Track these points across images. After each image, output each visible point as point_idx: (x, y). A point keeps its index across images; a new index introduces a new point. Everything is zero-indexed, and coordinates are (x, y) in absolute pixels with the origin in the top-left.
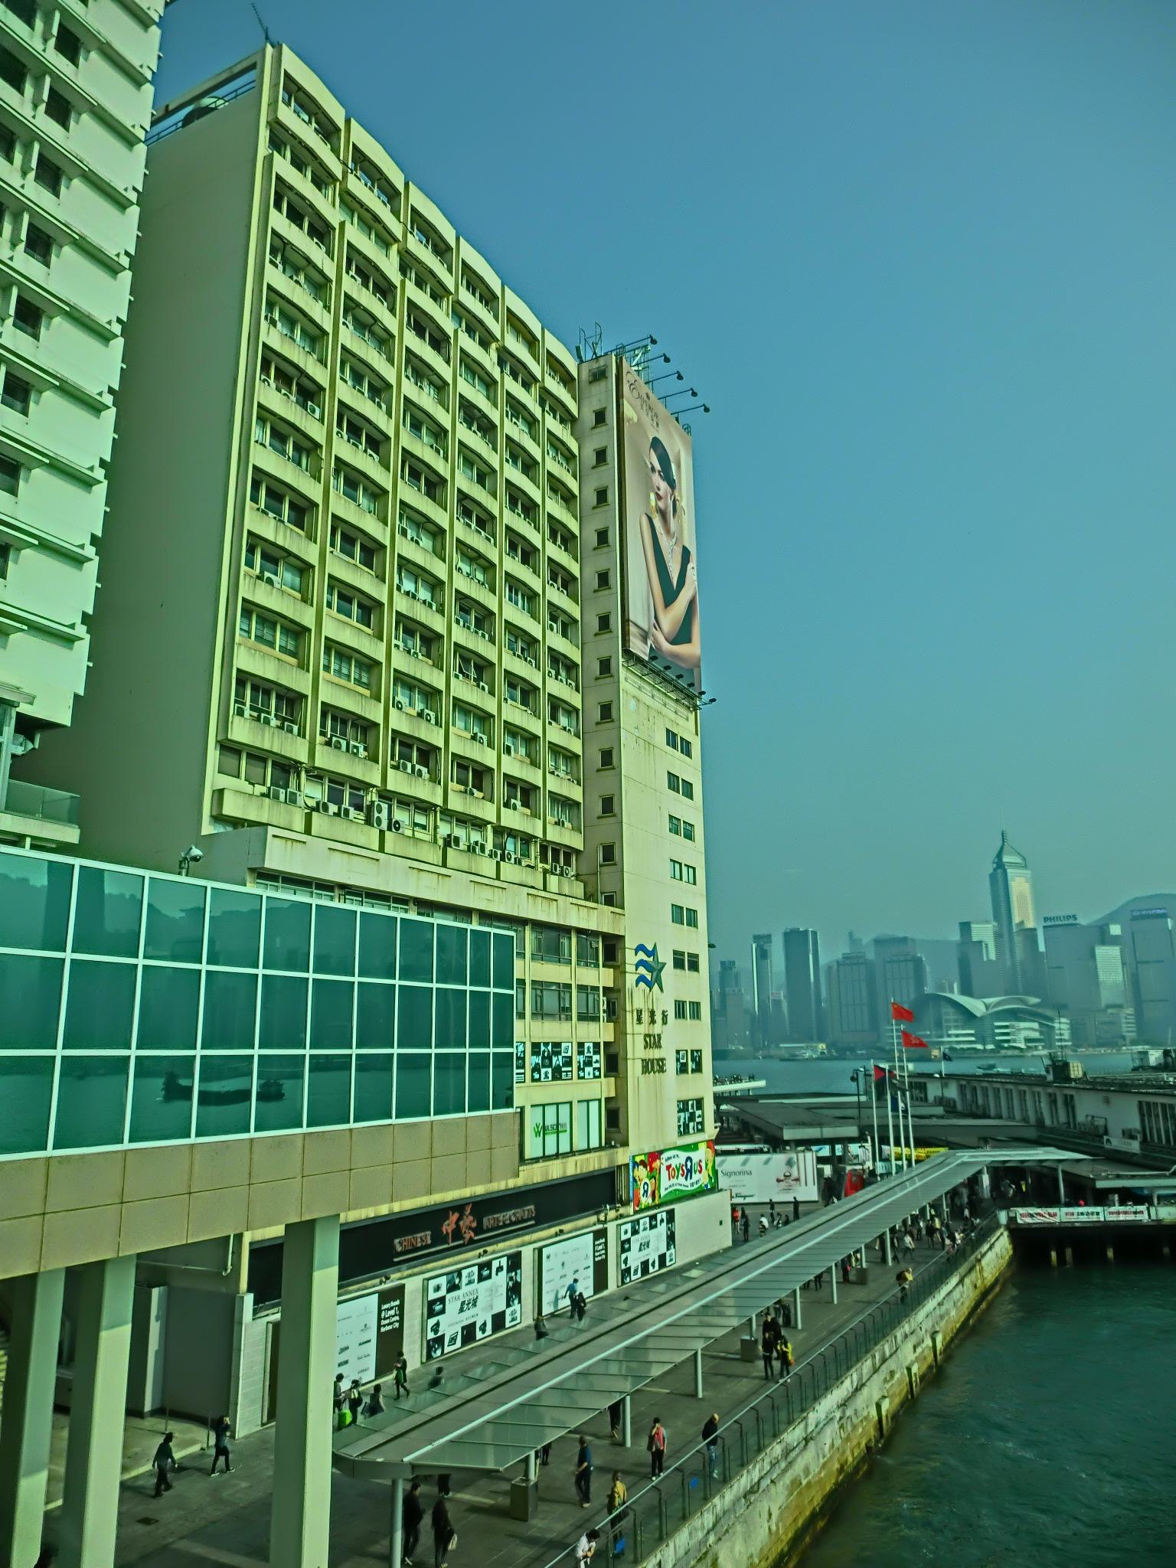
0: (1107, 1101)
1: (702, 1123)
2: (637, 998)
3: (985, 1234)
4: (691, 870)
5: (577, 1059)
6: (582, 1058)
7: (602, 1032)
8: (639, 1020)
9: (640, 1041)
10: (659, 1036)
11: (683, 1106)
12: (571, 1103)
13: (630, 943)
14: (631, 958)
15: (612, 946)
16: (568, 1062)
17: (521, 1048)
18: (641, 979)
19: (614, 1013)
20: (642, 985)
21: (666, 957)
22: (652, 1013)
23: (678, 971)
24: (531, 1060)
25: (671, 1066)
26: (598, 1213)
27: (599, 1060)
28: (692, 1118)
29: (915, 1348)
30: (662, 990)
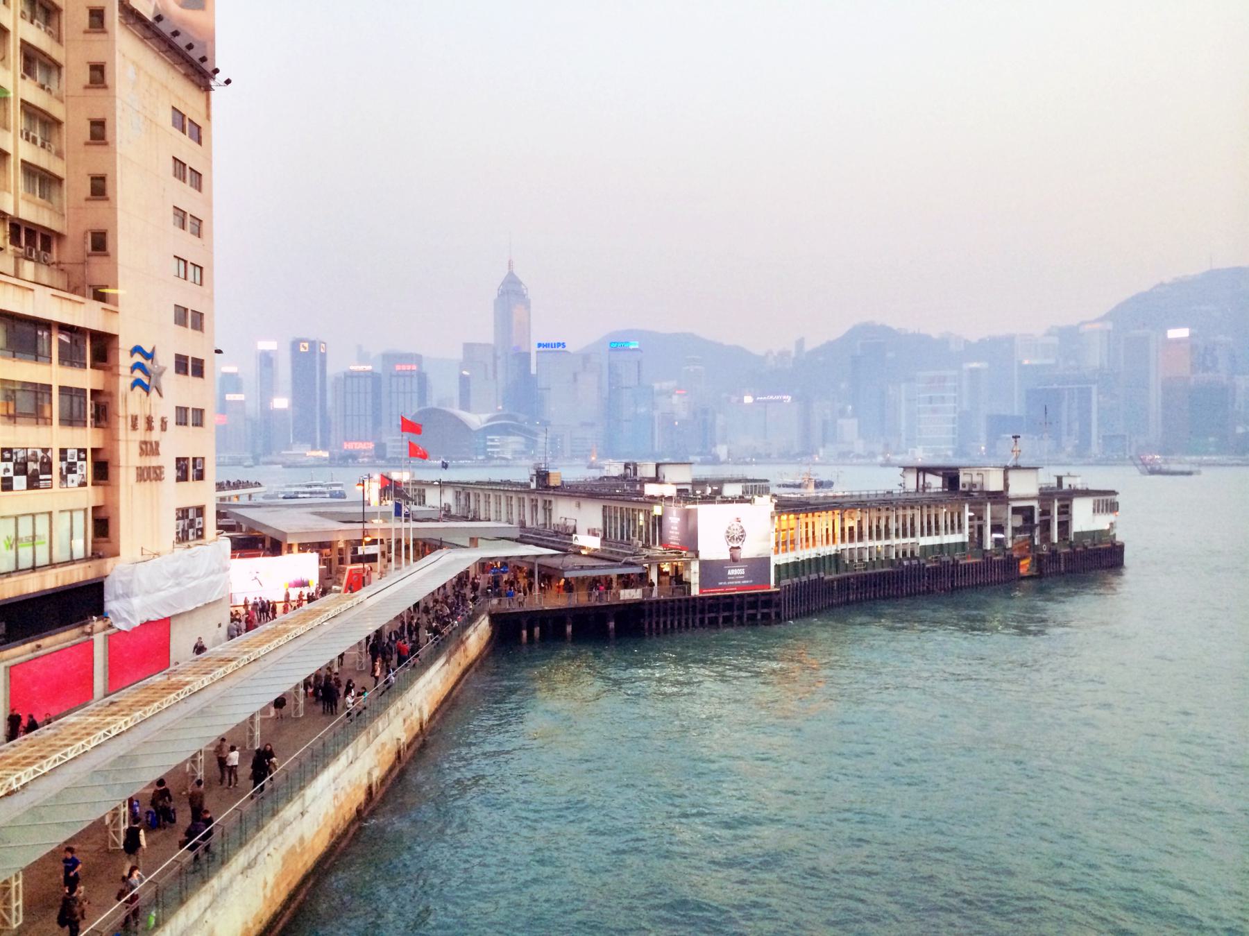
0: (579, 505)
1: (202, 530)
2: (130, 403)
3: (472, 619)
4: (198, 270)
7: (88, 437)
8: (134, 427)
9: (135, 449)
10: (157, 444)
11: (183, 513)
12: (50, 513)
13: (125, 344)
14: (125, 360)
18: (138, 383)
20: (138, 389)
21: (165, 360)
22: (149, 421)
23: (181, 377)
25: (171, 472)
26: (83, 625)
28: (191, 525)
29: (404, 721)
30: (161, 395)
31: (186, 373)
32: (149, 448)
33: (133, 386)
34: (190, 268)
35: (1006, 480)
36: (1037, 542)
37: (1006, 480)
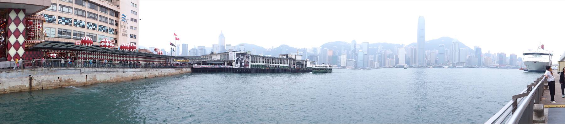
2: (121, 23)
5: (108, 30)
6: (110, 30)
7: (114, 27)
9: (122, 30)
14: (120, 16)
15: (117, 14)
16: (107, 30)
17: (96, 25)
18: (123, 20)
19: (117, 25)
24: (98, 28)
27: (114, 31)
31: (133, 21)
32: (124, 31)
33: (122, 21)
34: (135, 5)
35: (296, 57)
36: (301, 68)
37: (296, 57)
